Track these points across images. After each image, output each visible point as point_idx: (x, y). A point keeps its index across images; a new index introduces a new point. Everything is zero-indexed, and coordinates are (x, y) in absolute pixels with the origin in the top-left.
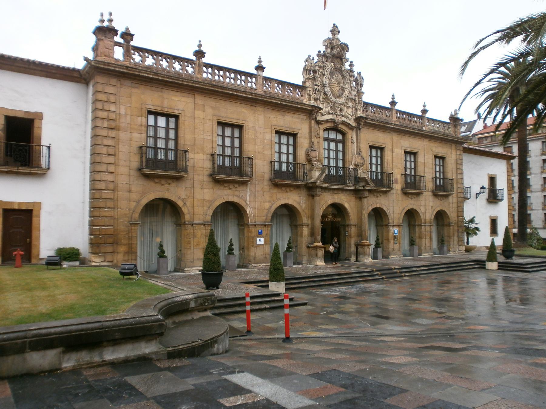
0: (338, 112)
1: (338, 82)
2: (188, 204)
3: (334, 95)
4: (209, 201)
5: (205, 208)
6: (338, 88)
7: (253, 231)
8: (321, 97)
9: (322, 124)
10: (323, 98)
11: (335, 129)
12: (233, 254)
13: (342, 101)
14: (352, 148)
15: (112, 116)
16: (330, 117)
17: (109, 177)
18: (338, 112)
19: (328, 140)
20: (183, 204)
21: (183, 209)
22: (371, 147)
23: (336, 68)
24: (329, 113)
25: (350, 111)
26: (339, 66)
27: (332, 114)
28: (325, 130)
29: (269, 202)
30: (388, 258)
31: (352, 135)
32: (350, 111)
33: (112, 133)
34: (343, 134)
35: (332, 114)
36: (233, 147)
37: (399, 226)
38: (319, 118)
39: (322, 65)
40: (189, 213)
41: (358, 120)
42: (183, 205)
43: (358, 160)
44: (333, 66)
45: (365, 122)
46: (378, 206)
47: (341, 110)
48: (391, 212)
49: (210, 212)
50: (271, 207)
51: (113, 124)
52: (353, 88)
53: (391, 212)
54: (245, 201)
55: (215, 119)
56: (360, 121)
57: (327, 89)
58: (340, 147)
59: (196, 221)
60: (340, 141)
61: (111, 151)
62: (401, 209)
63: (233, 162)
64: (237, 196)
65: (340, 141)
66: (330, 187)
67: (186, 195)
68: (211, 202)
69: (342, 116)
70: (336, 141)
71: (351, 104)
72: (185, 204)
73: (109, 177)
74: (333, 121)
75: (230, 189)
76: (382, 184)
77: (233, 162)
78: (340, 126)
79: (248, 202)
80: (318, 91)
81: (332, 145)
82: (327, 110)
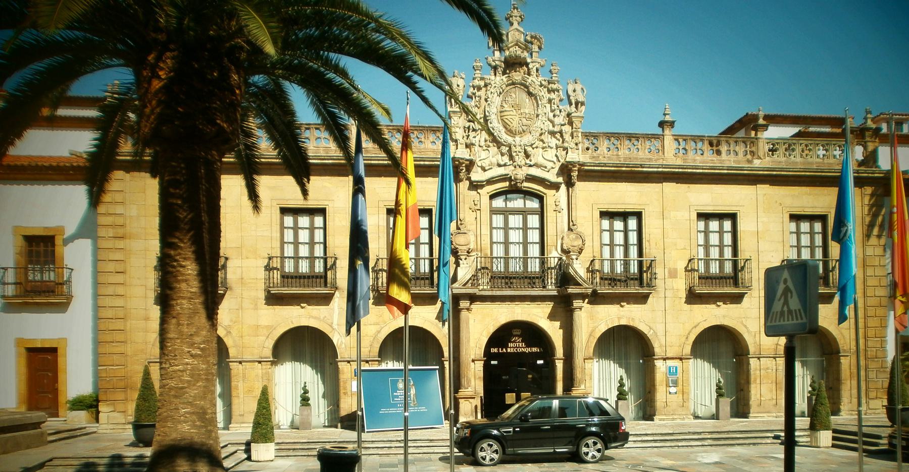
0: (520, 159)
1: (517, 107)
2: (234, 332)
3: (510, 132)
4: (267, 327)
5: (263, 338)
6: (517, 119)
7: (345, 370)
8: (483, 140)
9: (482, 187)
10: (486, 141)
11: (514, 190)
12: (309, 405)
13: (527, 139)
14: (556, 223)
15: (120, 221)
16: (501, 171)
17: (119, 302)
18: (520, 159)
19: (506, 212)
20: (225, 332)
21: (225, 340)
22: (604, 214)
23: (513, 84)
24: (499, 165)
25: (551, 154)
26: (520, 78)
27: (505, 165)
28: (492, 197)
29: (377, 324)
30: (653, 420)
31: (556, 199)
32: (551, 154)
33: (120, 244)
34: (541, 198)
35: (505, 165)
36: (312, 244)
37: (681, 359)
38: (477, 175)
39: (482, 83)
40: (235, 346)
41: (565, 170)
42: (226, 335)
43: (571, 242)
44: (505, 80)
45: (579, 171)
46: (623, 322)
47: (527, 156)
48: (661, 333)
49: (270, 344)
50: (379, 332)
51: (120, 232)
52: (557, 112)
53: (661, 333)
54: (331, 326)
55: (275, 203)
56: (570, 171)
57: (495, 124)
58: (534, 221)
59: (247, 357)
60: (532, 212)
61: (120, 267)
62: (688, 327)
63: (312, 266)
64: (315, 318)
65: (532, 212)
66: (499, 293)
67: (231, 321)
68: (271, 328)
69: (530, 166)
70: (524, 213)
71: (553, 142)
72: (229, 333)
73: (119, 302)
74: (504, 178)
75: (302, 308)
76: (636, 284)
77: (312, 266)
78: (526, 184)
79: (335, 326)
80: (474, 130)
81: (515, 221)
82: (494, 161)
